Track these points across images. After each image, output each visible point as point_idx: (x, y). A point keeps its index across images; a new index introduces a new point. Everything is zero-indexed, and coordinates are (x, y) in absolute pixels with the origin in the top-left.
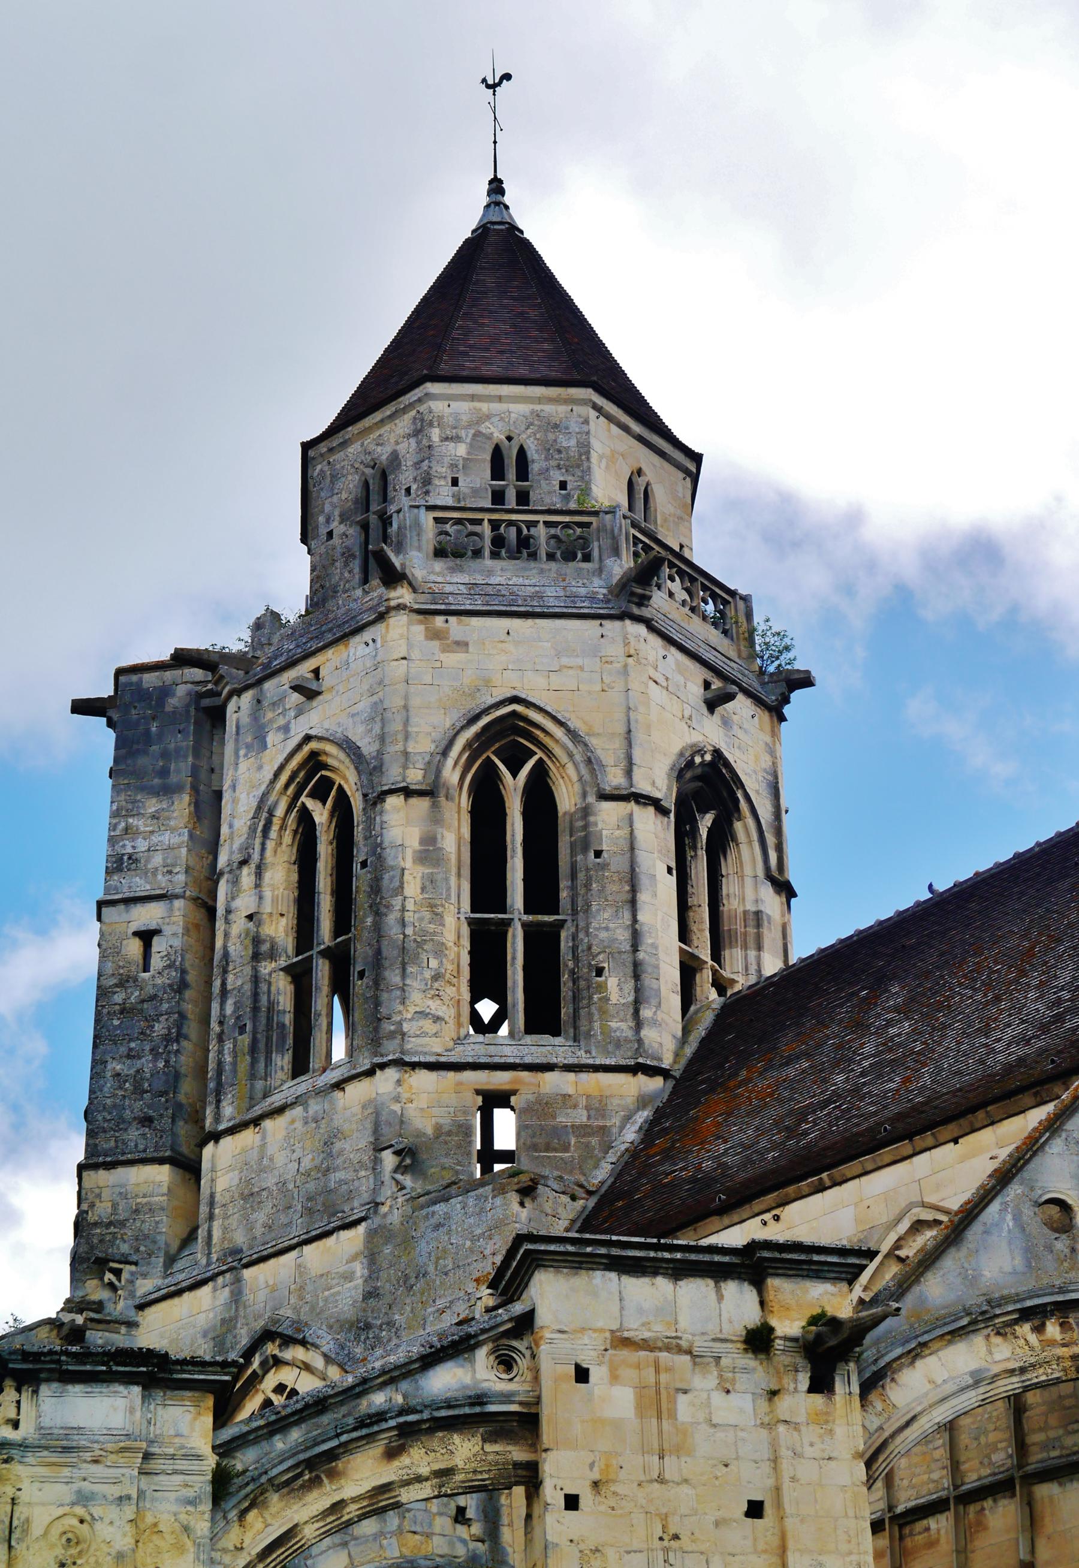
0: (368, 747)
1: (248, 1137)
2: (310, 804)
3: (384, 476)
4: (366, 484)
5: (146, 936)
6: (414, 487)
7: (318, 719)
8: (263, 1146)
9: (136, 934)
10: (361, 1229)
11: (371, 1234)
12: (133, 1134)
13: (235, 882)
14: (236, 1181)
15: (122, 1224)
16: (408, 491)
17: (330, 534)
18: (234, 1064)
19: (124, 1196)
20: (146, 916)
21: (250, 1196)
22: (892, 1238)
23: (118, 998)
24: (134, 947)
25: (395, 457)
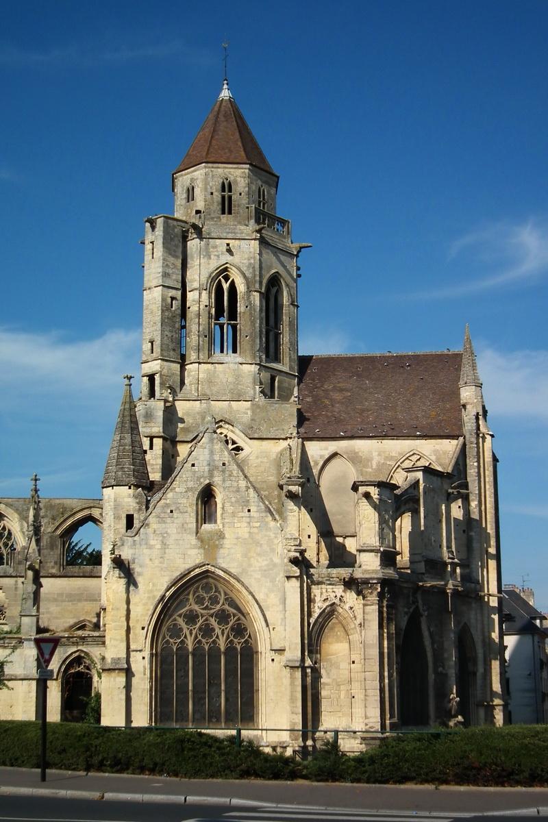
0: (248, 274)
2: (223, 280)
4: (223, 184)
5: (173, 298)
6: (243, 194)
7: (226, 258)
8: (215, 372)
9: (171, 297)
11: (253, 405)
12: (172, 353)
15: (170, 376)
16: (240, 194)
17: (212, 194)
19: (170, 369)
20: (172, 293)
21: (210, 382)
22: (408, 455)
23: (166, 314)
24: (169, 300)
25: (236, 181)
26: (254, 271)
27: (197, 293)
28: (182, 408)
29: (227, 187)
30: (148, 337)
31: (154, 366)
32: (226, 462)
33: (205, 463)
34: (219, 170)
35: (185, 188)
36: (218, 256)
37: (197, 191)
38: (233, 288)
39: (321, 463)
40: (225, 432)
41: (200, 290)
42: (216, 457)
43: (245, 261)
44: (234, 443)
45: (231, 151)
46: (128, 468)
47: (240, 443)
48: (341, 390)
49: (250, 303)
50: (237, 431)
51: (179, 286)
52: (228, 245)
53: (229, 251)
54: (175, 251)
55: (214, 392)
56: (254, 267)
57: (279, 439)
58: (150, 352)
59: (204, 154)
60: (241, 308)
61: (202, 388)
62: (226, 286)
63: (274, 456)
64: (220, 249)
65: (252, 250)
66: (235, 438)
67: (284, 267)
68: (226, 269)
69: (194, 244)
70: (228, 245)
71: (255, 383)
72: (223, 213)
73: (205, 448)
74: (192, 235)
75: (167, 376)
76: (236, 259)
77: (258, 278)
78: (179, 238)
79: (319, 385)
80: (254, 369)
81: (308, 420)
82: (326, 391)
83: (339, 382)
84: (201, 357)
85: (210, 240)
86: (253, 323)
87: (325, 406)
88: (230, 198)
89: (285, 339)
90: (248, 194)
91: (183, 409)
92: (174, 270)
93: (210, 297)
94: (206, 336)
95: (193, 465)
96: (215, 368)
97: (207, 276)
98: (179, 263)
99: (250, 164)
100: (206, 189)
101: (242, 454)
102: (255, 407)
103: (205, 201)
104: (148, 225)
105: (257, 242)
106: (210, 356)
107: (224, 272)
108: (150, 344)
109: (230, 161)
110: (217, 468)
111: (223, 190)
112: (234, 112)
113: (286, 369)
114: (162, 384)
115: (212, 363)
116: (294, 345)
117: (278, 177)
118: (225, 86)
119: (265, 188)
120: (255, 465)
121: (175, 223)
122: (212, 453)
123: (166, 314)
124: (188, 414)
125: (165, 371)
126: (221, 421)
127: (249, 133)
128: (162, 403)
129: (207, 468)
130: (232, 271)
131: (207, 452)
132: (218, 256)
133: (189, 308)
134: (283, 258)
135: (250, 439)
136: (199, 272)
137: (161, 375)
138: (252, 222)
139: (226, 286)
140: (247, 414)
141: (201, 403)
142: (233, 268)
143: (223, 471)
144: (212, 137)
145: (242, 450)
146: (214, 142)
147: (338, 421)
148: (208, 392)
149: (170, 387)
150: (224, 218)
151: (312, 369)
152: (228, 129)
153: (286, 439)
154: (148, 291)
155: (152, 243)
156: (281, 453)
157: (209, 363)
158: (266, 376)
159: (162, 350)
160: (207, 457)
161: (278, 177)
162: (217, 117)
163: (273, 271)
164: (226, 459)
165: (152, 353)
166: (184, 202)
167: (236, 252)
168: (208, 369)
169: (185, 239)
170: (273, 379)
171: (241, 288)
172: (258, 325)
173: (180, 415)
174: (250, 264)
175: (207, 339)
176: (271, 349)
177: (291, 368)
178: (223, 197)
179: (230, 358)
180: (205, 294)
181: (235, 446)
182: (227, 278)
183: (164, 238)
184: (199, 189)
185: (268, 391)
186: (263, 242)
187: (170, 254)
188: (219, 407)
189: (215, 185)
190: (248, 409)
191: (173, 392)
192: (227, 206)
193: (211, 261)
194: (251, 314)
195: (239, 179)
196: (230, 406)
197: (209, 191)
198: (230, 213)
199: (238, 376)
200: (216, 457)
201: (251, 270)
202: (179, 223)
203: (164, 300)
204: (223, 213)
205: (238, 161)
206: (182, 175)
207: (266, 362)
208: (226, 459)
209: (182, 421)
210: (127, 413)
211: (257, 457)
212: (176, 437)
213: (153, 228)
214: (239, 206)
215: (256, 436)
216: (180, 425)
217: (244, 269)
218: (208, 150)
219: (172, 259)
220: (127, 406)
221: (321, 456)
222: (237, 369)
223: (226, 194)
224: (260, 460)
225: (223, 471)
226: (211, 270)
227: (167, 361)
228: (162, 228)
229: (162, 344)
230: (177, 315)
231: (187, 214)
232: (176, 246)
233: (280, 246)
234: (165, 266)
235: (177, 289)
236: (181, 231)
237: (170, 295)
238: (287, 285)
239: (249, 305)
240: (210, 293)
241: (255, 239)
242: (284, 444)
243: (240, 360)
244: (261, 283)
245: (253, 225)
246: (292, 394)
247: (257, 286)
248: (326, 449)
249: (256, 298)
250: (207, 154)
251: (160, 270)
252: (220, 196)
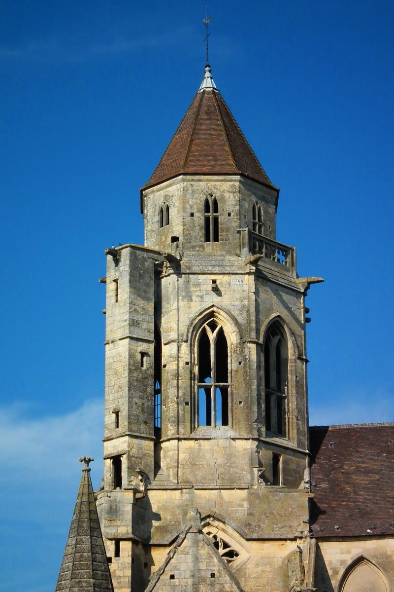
0: (241, 320)
1: (192, 443)
2: (208, 329)
3: (215, 203)
4: (207, 202)
5: (143, 354)
6: (232, 214)
8: (199, 450)
9: (141, 352)
10: (246, 491)
11: (250, 494)
12: (143, 427)
13: (179, 347)
14: (188, 457)
15: (141, 458)
16: (229, 215)
17: (192, 215)
18: (184, 415)
19: (141, 448)
20: (143, 347)
21: (193, 464)
23: (135, 375)
24: (139, 356)
25: (223, 197)
26: (249, 315)
27: (174, 346)
28: (157, 499)
29: (211, 206)
30: (112, 407)
31: (120, 445)
32: (216, 573)
33: (188, 574)
34: (201, 183)
35: (157, 208)
36: (202, 297)
37: (173, 212)
38: (221, 339)
39: (342, 572)
40: (214, 531)
41: (179, 342)
42: (203, 566)
43: (237, 303)
44: (226, 546)
45: (216, 159)
46: (86, 582)
47: (235, 546)
48: (367, 472)
49: (243, 357)
50: (230, 530)
51: (152, 337)
52: (214, 282)
53: (216, 290)
54: (145, 292)
55: (199, 478)
56: (248, 311)
57: (285, 540)
58: (114, 426)
59: (182, 163)
60: (232, 364)
61: (184, 473)
62: (212, 336)
63: (279, 562)
64: (204, 287)
65: (246, 288)
66: (227, 540)
67: (289, 309)
68: (212, 314)
69: (169, 282)
70: (214, 282)
71: (252, 465)
72: (207, 239)
73: (188, 554)
74: (167, 269)
75: (137, 458)
76: (225, 301)
77: (253, 325)
78: (150, 274)
79: (336, 466)
80: (251, 445)
81: (324, 513)
82: (347, 473)
83: (363, 462)
84: (181, 431)
85: (191, 276)
86: (249, 384)
87: (346, 494)
88: (216, 220)
89: (291, 404)
90: (240, 213)
91: (159, 502)
92: (144, 317)
93: (191, 352)
94: (187, 404)
95: (172, 577)
96: (200, 445)
97: (188, 323)
98: (151, 307)
99: (242, 175)
100: (184, 209)
101: (237, 561)
102: (254, 497)
103: (184, 225)
104: (110, 258)
105: (252, 277)
106: (193, 429)
107: (209, 318)
108: (114, 415)
109: (215, 171)
110: (203, 580)
111: (207, 209)
112: (220, 107)
113: (293, 445)
114: (131, 468)
115: (196, 439)
116: (303, 414)
117: (278, 191)
118: (208, 74)
119: (261, 205)
120: (254, 575)
121: (145, 254)
122: (196, 560)
123: (135, 375)
124: (165, 508)
125: (134, 451)
126: (209, 516)
127: (240, 135)
128: (130, 495)
129: (190, 581)
130: (219, 316)
131: (190, 558)
132: (202, 297)
133: (165, 366)
134: (285, 297)
135: (248, 540)
136: (178, 319)
137: (129, 457)
138: (246, 250)
139: (212, 336)
140: (242, 506)
141: (182, 493)
142: (222, 312)
143: (212, 585)
144: (192, 141)
145: (237, 555)
146: (194, 147)
147: (364, 514)
148: (191, 479)
149: (141, 473)
150: (209, 247)
151: (328, 445)
152: (213, 128)
153: (295, 539)
154: (111, 345)
155: (116, 281)
156: (289, 560)
157: (192, 439)
158: (266, 455)
159: (129, 423)
160: (191, 565)
161: (278, 191)
162: (197, 114)
163: (274, 315)
164: (216, 568)
165: (117, 427)
166: (156, 226)
167: (223, 292)
168: (190, 448)
169: (158, 275)
170: (276, 459)
171: (232, 338)
172: (254, 387)
173: (155, 509)
174: (244, 306)
175: (188, 407)
176: (272, 418)
177: (300, 444)
178: (207, 220)
179: (219, 431)
180: (185, 348)
181: (227, 550)
182: (213, 326)
183: (131, 275)
184: (176, 210)
185: (269, 475)
186: (260, 277)
187: (139, 295)
188: (206, 498)
189: (196, 203)
190: (244, 500)
191: (146, 479)
192: (212, 231)
193: (193, 304)
194: (245, 372)
195: (227, 195)
196: (220, 496)
197: (189, 211)
198: (216, 239)
199: (230, 456)
200: (203, 566)
201: (245, 314)
202: (150, 255)
203: (131, 356)
204: (207, 239)
205: (225, 171)
206: (153, 192)
207: (267, 436)
208: (216, 568)
209: (158, 517)
210: (85, 508)
211: (257, 565)
212: (149, 538)
213: (117, 261)
214: (228, 230)
215: (255, 536)
216: (155, 523)
217: (236, 313)
218: (186, 158)
219: (141, 303)
220: (85, 499)
221: (342, 562)
222: (230, 445)
223: (211, 215)
224: (260, 569)
225: (212, 585)
226: (192, 316)
227: (136, 437)
228: (128, 262)
229: (129, 416)
230: (149, 376)
231: (161, 243)
232: (147, 285)
233: (282, 281)
234: (133, 311)
235: (148, 341)
236: (153, 265)
237: (140, 349)
238: (293, 334)
239: (243, 361)
240: (192, 346)
241: (249, 274)
242: (291, 546)
243: (232, 434)
244: (258, 331)
245: (246, 255)
246: (302, 478)
247: (253, 335)
248: (349, 552)
249: (252, 351)
250: (186, 162)
251: (127, 317)
252: (203, 218)
